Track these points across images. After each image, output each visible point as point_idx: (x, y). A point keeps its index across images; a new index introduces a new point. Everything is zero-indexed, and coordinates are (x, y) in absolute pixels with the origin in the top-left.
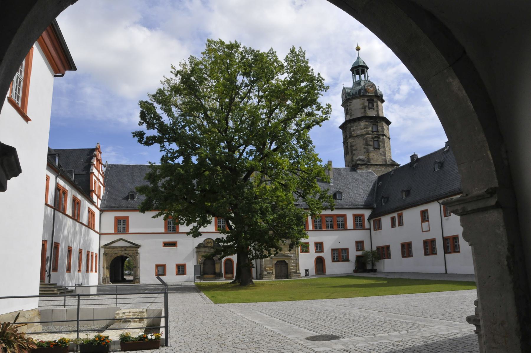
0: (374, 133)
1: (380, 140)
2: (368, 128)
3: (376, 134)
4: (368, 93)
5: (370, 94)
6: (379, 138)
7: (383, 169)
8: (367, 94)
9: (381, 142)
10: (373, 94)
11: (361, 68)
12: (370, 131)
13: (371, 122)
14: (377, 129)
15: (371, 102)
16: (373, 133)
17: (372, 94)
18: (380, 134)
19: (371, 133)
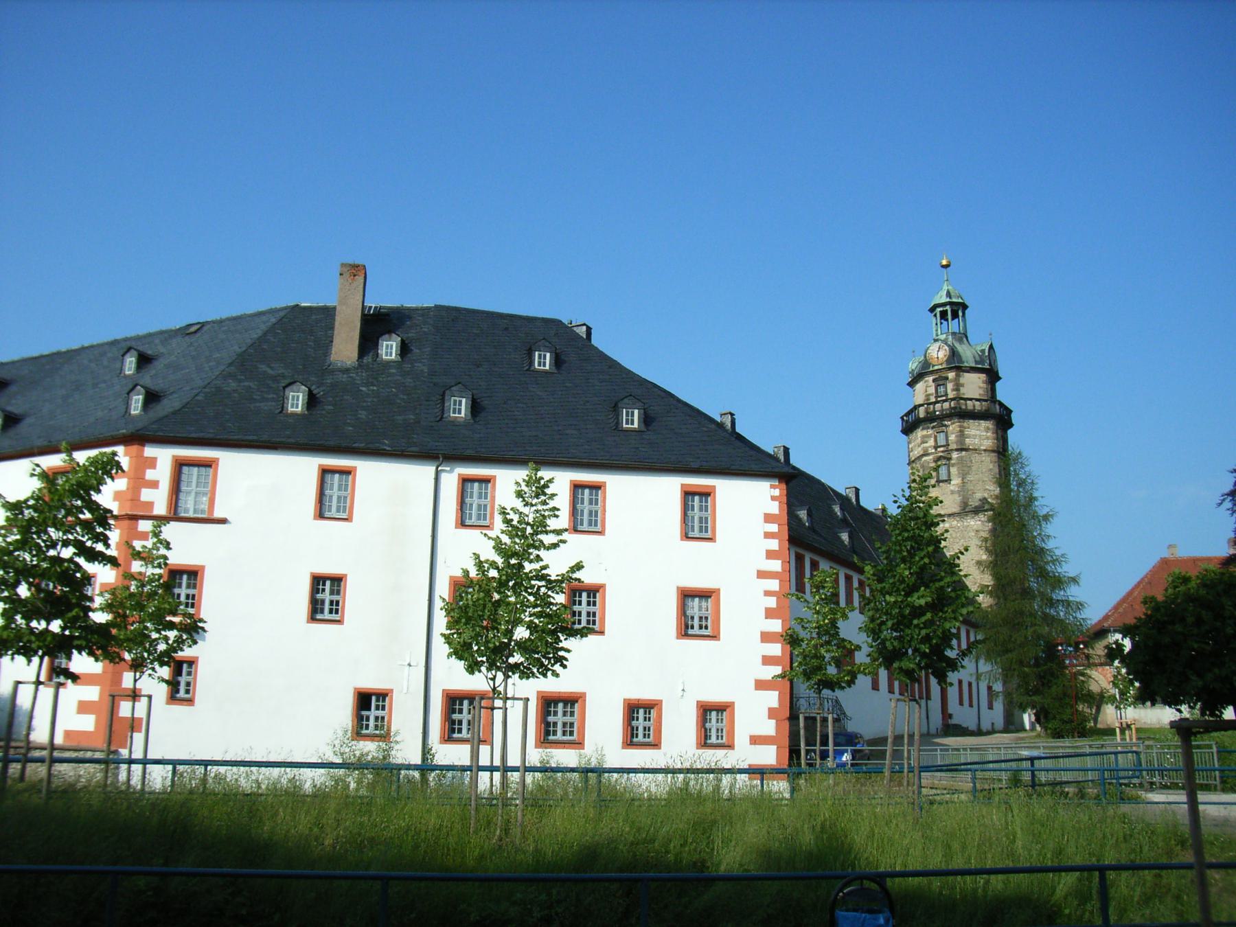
0: (939, 449)
1: (952, 462)
2: (927, 442)
3: (942, 452)
4: (933, 366)
5: (936, 368)
6: (949, 459)
7: (955, 523)
8: (931, 369)
9: (953, 465)
10: (944, 366)
11: (941, 309)
12: (930, 447)
13: (933, 428)
14: (947, 439)
15: (941, 382)
16: (936, 450)
17: (940, 367)
18: (952, 450)
19: (933, 451)
